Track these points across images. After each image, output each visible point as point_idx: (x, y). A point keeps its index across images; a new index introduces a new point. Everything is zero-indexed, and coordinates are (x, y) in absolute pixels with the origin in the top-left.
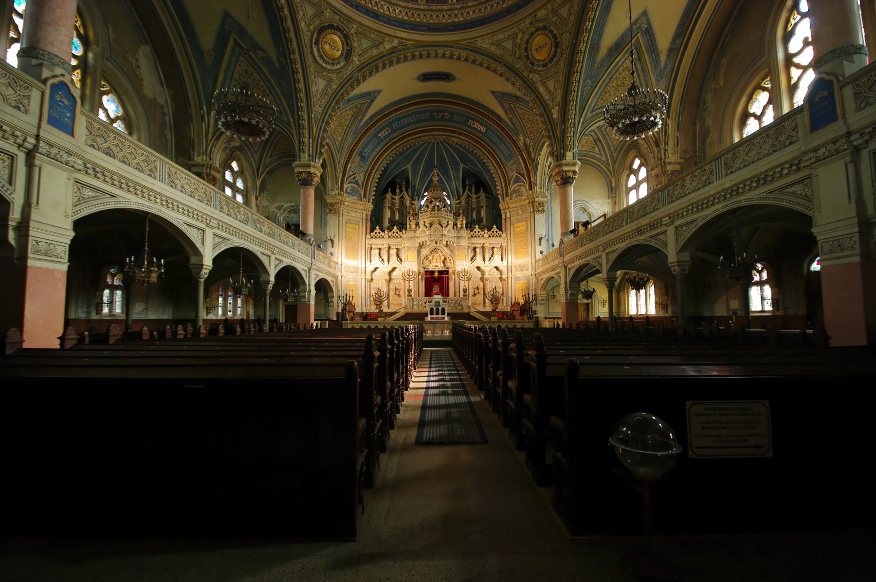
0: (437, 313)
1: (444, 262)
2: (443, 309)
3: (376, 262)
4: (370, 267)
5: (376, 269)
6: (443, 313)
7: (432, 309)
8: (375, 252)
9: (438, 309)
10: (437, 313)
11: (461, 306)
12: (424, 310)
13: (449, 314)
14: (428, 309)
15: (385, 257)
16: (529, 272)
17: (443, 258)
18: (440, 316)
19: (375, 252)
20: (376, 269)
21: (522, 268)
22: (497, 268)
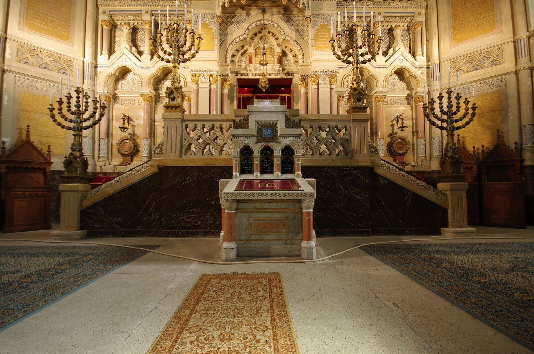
0: (267, 168)
1: (280, 62)
2: (288, 151)
3: (124, 56)
4: (108, 65)
5: (124, 72)
6: (288, 166)
7: (246, 152)
8: (123, 36)
9: (267, 152)
10: (267, 168)
11: (346, 142)
12: (212, 156)
13: (307, 172)
14: (231, 153)
15: (146, 46)
16: (508, 65)
17: (278, 51)
18: (277, 174)
19: (123, 36)
20: (124, 72)
21: (490, 56)
22: (400, 73)
